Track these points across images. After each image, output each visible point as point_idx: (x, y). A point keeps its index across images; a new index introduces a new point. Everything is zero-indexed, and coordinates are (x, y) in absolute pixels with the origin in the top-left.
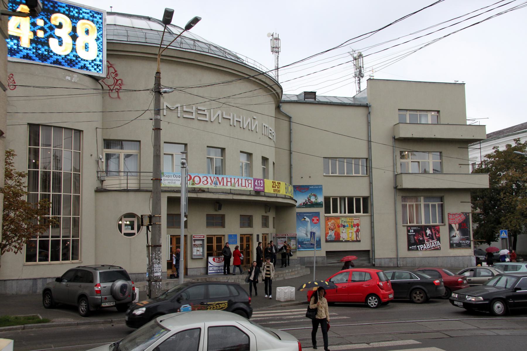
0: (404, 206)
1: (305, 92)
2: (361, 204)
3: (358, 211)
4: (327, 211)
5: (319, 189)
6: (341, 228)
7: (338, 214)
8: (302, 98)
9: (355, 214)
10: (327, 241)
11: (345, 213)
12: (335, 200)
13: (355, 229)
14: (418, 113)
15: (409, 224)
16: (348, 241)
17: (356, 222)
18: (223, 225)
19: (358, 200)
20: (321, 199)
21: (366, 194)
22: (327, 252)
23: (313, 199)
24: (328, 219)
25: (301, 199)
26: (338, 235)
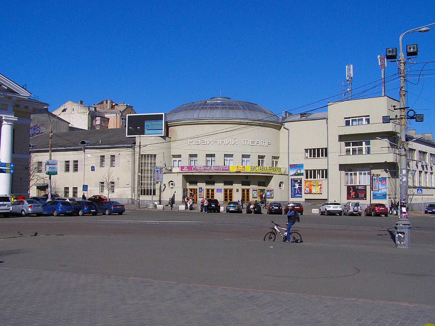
2: (325, 173)
3: (311, 178)
4: (307, 178)
5: (301, 166)
6: (313, 187)
7: (312, 179)
9: (309, 179)
10: (305, 193)
12: (311, 171)
13: (319, 187)
14: (357, 118)
16: (316, 194)
17: (320, 184)
20: (303, 171)
23: (299, 172)
24: (306, 182)
25: (292, 172)
26: (310, 190)
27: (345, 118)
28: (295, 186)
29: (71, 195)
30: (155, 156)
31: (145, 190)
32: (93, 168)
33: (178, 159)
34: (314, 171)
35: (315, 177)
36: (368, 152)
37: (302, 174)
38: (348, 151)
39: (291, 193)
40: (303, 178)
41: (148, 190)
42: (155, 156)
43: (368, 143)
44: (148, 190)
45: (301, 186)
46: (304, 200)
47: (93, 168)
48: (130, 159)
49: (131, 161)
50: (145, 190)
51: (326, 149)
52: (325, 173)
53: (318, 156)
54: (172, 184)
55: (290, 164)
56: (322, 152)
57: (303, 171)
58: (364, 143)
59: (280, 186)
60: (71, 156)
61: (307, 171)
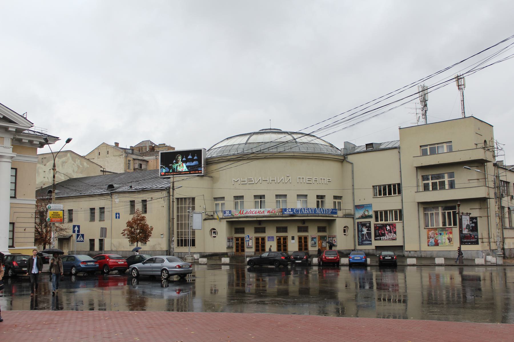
0: (426, 215)
1: (366, 145)
2: (399, 214)
4: (377, 220)
5: (370, 206)
8: (365, 149)
11: (393, 220)
14: (436, 146)
15: (430, 227)
18: (264, 231)
19: (381, 213)
21: (400, 208)
22: (376, 247)
23: (366, 213)
27: (421, 146)
28: (362, 231)
29: (97, 247)
30: (193, 199)
31: (182, 240)
32: (118, 215)
33: (220, 202)
34: (386, 212)
35: (386, 220)
36: (452, 185)
37: (370, 217)
38: (426, 188)
39: (358, 240)
40: (373, 221)
41: (185, 240)
42: (193, 199)
43: (451, 175)
44: (185, 240)
45: (370, 230)
46: (374, 248)
47: (118, 215)
48: (165, 204)
49: (165, 206)
50: (182, 240)
51: (399, 185)
52: (399, 214)
53: (390, 193)
54: (214, 232)
55: (356, 204)
56: (394, 189)
57: (371, 213)
58: (446, 176)
59: (344, 231)
60: (97, 203)
61: (376, 212)
